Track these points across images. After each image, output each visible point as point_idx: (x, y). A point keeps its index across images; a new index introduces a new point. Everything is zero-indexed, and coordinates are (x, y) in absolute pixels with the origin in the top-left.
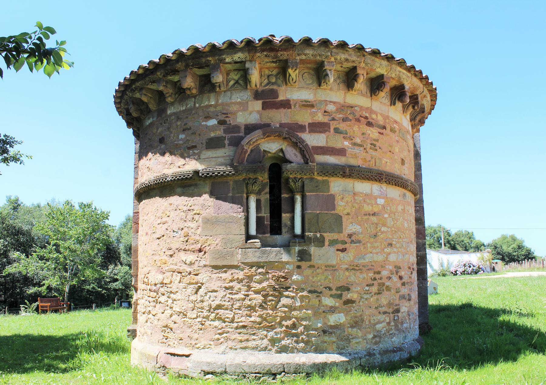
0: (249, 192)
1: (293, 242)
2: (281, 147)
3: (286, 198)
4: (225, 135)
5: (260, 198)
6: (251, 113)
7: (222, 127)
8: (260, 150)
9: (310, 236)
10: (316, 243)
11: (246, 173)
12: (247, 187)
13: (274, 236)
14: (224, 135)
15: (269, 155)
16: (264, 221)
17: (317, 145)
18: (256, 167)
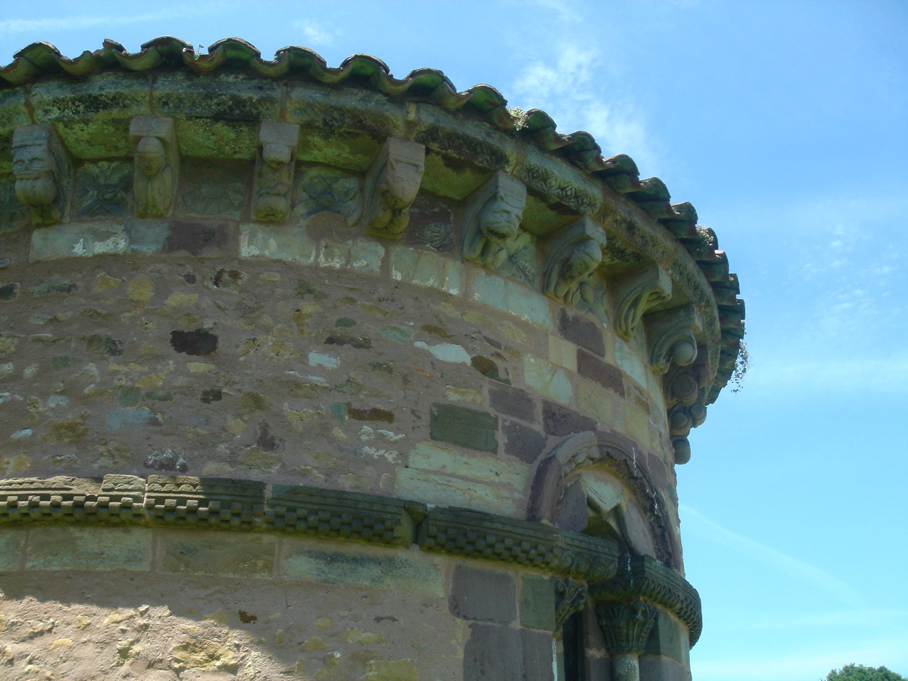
4: (497, 414)
6: (555, 368)
7: (487, 385)
14: (492, 412)
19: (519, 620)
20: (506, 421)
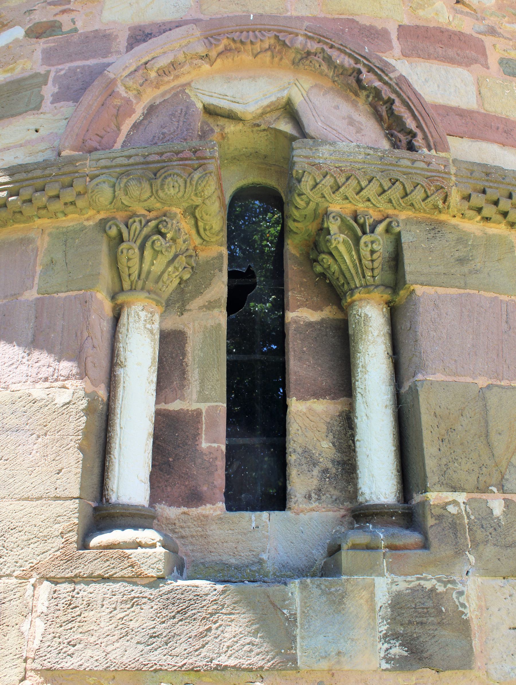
0: (126, 285)
1: (354, 547)
2: (285, 94)
3: (310, 325)
4: (48, 68)
5: (181, 327)
8: (190, 105)
9: (452, 509)
10: (489, 551)
11: (114, 186)
12: (115, 261)
13: (247, 514)
14: (42, 70)
15: (231, 128)
16: (196, 436)
17: (441, 101)
18: (161, 154)
19: (36, 288)
20: (61, 70)
